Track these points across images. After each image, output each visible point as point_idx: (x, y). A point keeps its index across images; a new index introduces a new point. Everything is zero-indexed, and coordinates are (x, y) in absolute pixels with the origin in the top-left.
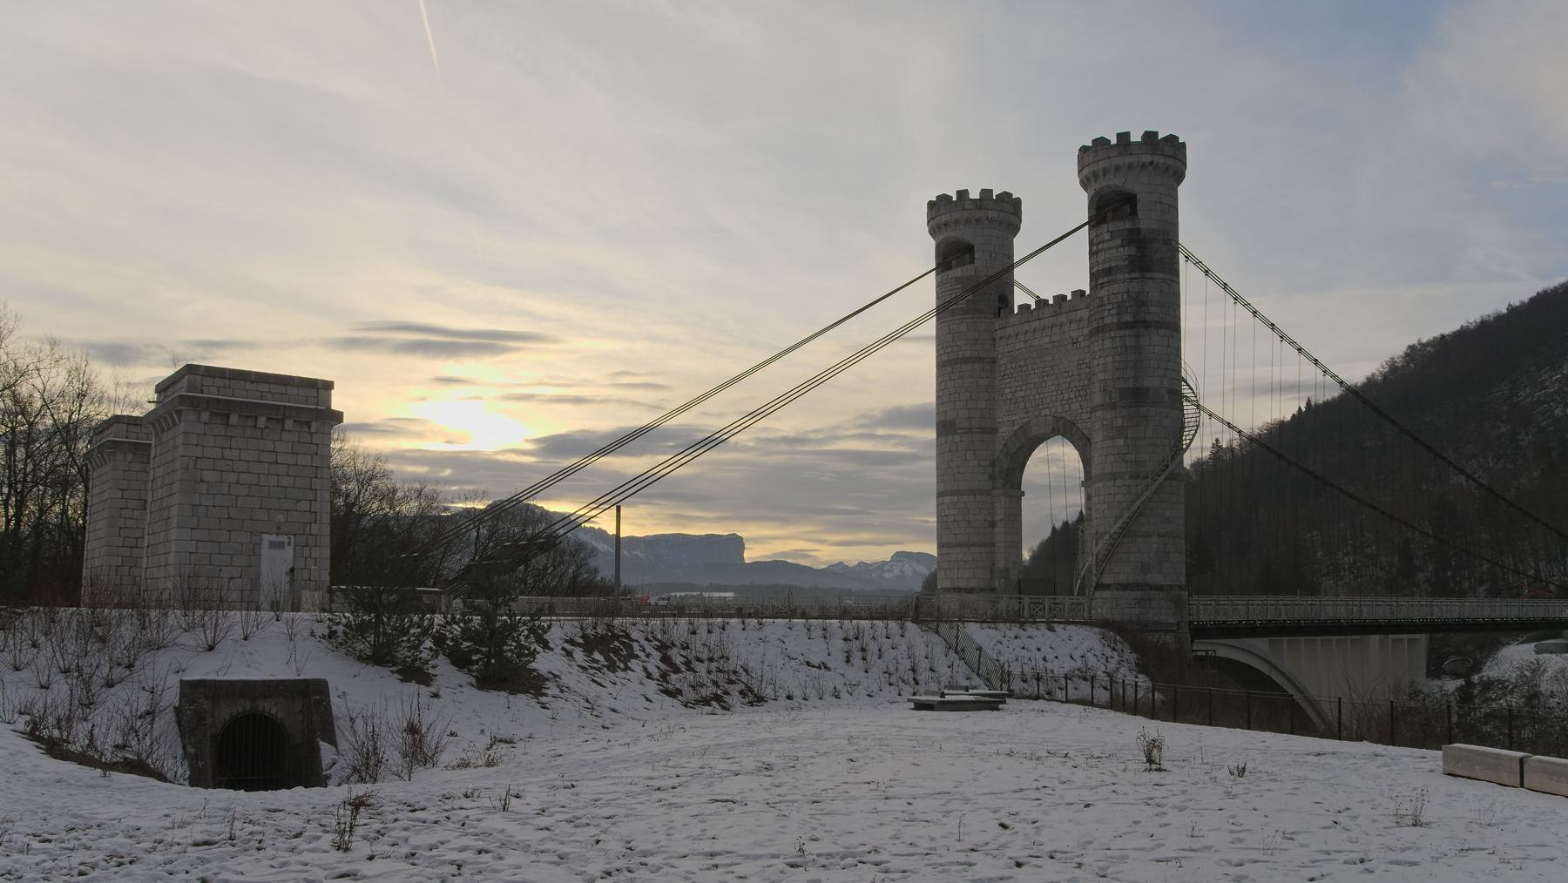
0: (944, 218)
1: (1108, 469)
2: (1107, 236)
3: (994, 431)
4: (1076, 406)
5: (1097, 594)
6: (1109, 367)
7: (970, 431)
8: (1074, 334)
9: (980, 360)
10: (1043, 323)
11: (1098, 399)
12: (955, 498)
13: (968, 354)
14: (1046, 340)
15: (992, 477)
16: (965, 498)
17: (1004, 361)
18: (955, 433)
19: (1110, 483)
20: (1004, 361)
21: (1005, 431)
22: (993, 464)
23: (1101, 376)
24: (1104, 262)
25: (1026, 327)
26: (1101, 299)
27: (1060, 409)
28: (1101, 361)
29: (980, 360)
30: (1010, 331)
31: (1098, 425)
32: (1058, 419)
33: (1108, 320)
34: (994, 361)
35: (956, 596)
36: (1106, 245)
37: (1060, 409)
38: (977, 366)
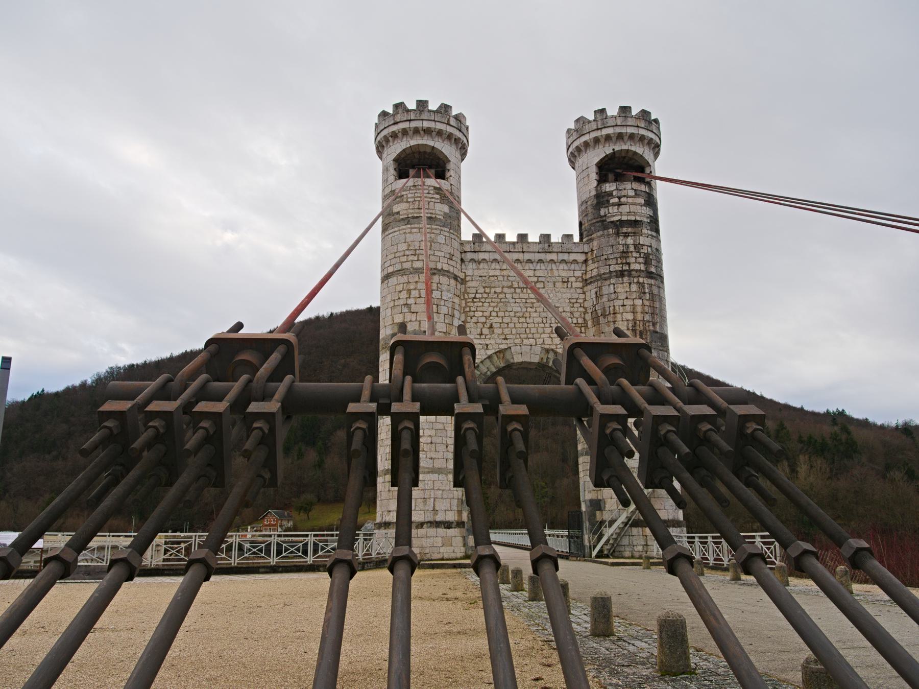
0: (426, 124)
2: (632, 193)
5: (635, 531)
6: (639, 309)
8: (565, 274)
13: (446, 268)
14: (531, 273)
23: (630, 316)
24: (629, 213)
27: (548, 341)
28: (627, 302)
30: (482, 256)
32: (548, 351)
34: (463, 282)
35: (432, 531)
36: (630, 200)
37: (548, 341)
38: (453, 282)
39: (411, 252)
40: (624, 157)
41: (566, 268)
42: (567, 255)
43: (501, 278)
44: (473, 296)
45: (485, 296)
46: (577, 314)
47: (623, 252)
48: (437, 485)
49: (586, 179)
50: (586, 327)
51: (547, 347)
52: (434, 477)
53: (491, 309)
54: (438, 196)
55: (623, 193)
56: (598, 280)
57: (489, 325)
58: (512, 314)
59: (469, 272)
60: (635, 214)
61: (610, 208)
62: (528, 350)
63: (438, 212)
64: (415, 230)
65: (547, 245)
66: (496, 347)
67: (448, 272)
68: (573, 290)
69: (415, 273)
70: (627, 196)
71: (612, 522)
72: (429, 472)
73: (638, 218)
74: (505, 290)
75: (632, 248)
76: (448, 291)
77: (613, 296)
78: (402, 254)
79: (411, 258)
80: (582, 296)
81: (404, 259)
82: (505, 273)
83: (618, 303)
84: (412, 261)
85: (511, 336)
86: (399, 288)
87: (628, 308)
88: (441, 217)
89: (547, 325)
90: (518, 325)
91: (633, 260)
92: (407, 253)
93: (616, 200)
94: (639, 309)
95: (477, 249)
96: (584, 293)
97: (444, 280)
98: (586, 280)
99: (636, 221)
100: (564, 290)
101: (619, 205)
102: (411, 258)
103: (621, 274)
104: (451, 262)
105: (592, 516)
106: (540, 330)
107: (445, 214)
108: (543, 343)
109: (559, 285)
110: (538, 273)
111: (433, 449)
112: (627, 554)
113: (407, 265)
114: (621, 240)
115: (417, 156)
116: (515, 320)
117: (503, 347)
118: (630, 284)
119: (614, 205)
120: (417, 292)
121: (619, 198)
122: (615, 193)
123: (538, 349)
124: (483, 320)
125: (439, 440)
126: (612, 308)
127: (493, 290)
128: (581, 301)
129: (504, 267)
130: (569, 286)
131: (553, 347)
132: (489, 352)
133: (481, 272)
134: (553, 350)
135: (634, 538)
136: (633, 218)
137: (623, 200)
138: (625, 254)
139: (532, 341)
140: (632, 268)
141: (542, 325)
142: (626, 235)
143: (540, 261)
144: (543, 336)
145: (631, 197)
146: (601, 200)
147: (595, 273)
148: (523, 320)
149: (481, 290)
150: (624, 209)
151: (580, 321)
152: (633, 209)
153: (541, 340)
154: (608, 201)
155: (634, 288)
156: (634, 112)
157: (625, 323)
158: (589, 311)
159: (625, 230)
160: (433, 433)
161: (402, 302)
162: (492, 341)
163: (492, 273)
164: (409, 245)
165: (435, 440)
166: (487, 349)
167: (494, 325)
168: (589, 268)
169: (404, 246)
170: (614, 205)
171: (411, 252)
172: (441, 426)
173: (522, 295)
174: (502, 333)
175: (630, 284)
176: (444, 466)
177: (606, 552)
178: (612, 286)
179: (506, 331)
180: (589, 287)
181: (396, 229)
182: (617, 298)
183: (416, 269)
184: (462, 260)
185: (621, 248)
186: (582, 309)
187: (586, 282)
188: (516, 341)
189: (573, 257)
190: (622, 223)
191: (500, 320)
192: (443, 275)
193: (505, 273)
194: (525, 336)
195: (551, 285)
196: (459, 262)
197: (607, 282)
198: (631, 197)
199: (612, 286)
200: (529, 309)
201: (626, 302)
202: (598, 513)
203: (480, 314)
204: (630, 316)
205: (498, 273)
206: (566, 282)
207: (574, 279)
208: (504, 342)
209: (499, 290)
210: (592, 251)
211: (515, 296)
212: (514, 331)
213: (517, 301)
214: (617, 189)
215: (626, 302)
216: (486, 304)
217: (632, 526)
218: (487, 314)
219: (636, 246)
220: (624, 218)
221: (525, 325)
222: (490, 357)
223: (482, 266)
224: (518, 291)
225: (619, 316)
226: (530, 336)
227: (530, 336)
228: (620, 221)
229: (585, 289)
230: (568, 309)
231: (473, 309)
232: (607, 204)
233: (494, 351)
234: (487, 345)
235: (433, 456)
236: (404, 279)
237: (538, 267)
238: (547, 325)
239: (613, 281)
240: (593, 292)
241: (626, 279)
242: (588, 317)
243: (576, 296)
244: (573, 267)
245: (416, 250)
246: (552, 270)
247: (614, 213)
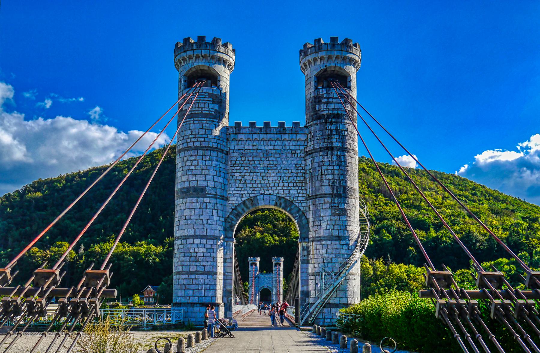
1: (335, 233)
3: (225, 199)
4: (295, 192)
5: (326, 310)
7: (215, 196)
8: (293, 148)
9: (222, 151)
10: (269, 136)
11: (327, 190)
12: (204, 241)
13: (215, 145)
14: (271, 147)
15: (225, 230)
16: (211, 242)
17: (235, 155)
18: (205, 197)
19: (337, 242)
20: (235, 155)
21: (234, 201)
22: (226, 220)
23: (330, 177)
24: (333, 110)
25: (255, 136)
26: (331, 131)
28: (330, 168)
29: (222, 151)
30: (240, 137)
31: (327, 206)
32: (280, 198)
33: (336, 144)
34: (227, 154)
36: (334, 100)
38: (220, 155)
39: (193, 136)
40: (334, 71)
41: (294, 144)
42: (295, 135)
43: (252, 151)
44: (234, 162)
45: (242, 162)
46: (300, 175)
48: (207, 281)
49: (309, 85)
50: (306, 183)
51: (281, 195)
52: (205, 277)
53: (245, 171)
54: (211, 100)
55: (331, 96)
57: (244, 182)
58: (259, 174)
59: (232, 147)
60: (338, 109)
61: (322, 105)
62: (268, 198)
63: (211, 110)
64: (196, 122)
65: (282, 129)
66: (248, 195)
67: (217, 148)
68: (298, 159)
69: (195, 149)
70: (332, 98)
71: (312, 304)
72: (201, 274)
73: (339, 112)
74: (255, 159)
75: (334, 133)
76: (217, 160)
77: (321, 164)
78: (188, 137)
79: (193, 140)
80: (303, 162)
81: (189, 140)
82: (255, 147)
83: (325, 168)
84: (194, 142)
85: (258, 189)
86: (186, 159)
87: (330, 172)
88: (213, 113)
89: (281, 181)
90: (262, 182)
91: (334, 140)
92: (191, 136)
93: (326, 100)
94: (336, 172)
96: (305, 160)
97: (214, 154)
98: (307, 152)
99: (338, 114)
100: (293, 159)
101: (328, 103)
102: (193, 140)
103: (327, 149)
104: (219, 142)
105: (304, 300)
106: (276, 185)
107: (216, 110)
108: (278, 193)
109: (289, 155)
110: (276, 148)
111: (204, 260)
112: (321, 323)
113: (190, 145)
114: (328, 126)
115: (200, 72)
116: (260, 178)
117: (251, 195)
118: (332, 155)
119: (325, 103)
120: (196, 162)
121: (328, 98)
122: (325, 96)
123: (274, 198)
124: (240, 178)
125: (209, 254)
126: (320, 172)
127: (247, 159)
128: (303, 166)
129: (255, 144)
130: (296, 156)
131: (283, 196)
132: (243, 199)
133: (239, 147)
134: (283, 198)
135: (326, 314)
136: (336, 112)
137: (330, 100)
138: (329, 137)
139: (271, 192)
140: (334, 145)
141: (277, 181)
142: (331, 123)
143: (277, 140)
144: (278, 188)
145: (336, 98)
146: (317, 100)
148: (265, 178)
149: (240, 159)
150: (332, 106)
151: (302, 178)
152: (336, 106)
153: (276, 192)
154: (321, 101)
155: (335, 158)
156: (340, 41)
157: (328, 181)
158: (308, 172)
159: (330, 120)
160: (204, 250)
161: (187, 168)
162: (246, 192)
163: (246, 147)
164: (192, 132)
165: (205, 254)
166: (242, 197)
167: (247, 182)
168: (309, 144)
169: (189, 132)
170: (325, 103)
171: (193, 136)
172: (209, 246)
173: (265, 162)
174: (252, 187)
175: (332, 155)
176: (211, 270)
177: (310, 322)
178: (321, 157)
179: (255, 185)
180: (308, 157)
182: (323, 165)
183: (196, 147)
184: (227, 139)
186: (303, 171)
187: (307, 153)
188: (261, 192)
189: (299, 136)
190: (329, 116)
191: (251, 178)
192: (213, 150)
194: (267, 189)
195: (284, 156)
196: (225, 140)
197: (318, 154)
198: (336, 98)
199: (321, 157)
200: (270, 171)
201: (329, 168)
202: (307, 298)
203: (238, 174)
204: (330, 177)
205: (250, 147)
206: (293, 153)
207: (299, 151)
208: (253, 192)
209: (250, 159)
210: (311, 133)
211: (261, 162)
212: (259, 186)
213: (262, 166)
214: (326, 93)
215: (329, 168)
216: (242, 168)
217: (324, 307)
218: (243, 174)
219: (337, 130)
220: (330, 112)
221: (267, 182)
222: (244, 203)
223: (240, 143)
224: (263, 159)
225: (324, 177)
226: (270, 188)
227: (270, 188)
229: (306, 158)
230: (294, 171)
231: (234, 171)
232: (320, 102)
233: (246, 198)
234: (242, 195)
235: (205, 264)
236: (188, 153)
237: (276, 144)
238: (281, 181)
239: (321, 154)
240: (310, 159)
241: (330, 152)
242: (307, 176)
243: (300, 162)
244: (299, 143)
245: (196, 135)
246: (285, 145)
247: (324, 109)
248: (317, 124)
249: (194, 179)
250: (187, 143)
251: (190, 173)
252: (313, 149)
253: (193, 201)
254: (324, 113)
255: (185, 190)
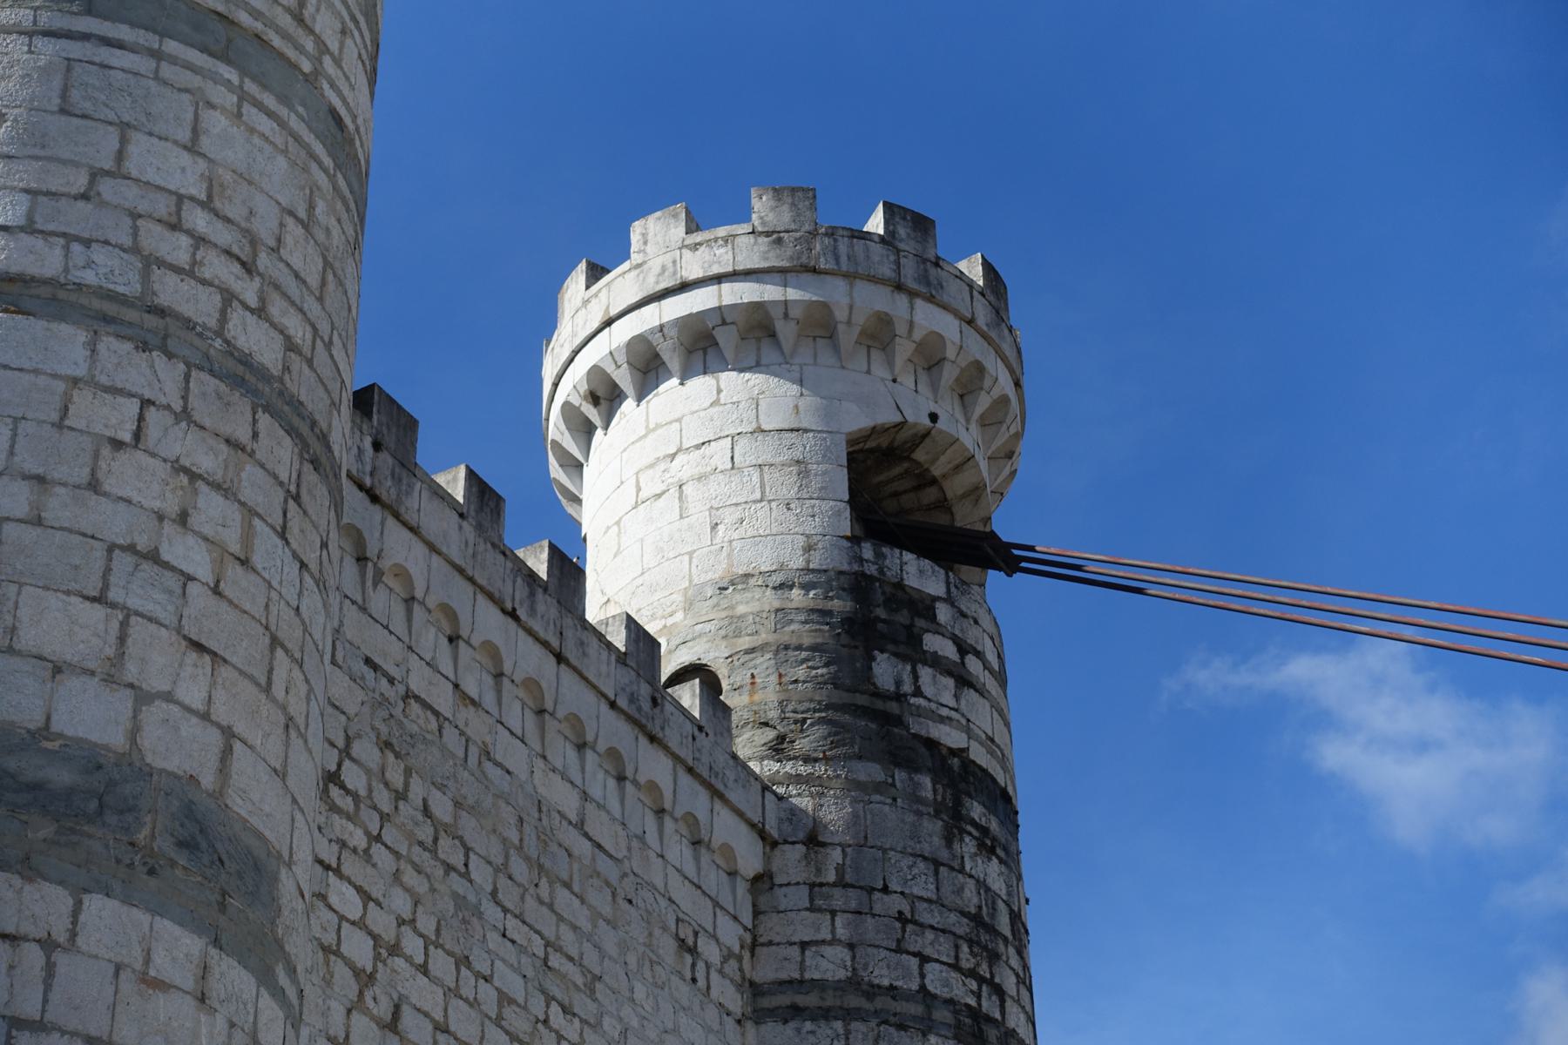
47: (976, 919)
56: (849, 1015)
57: (384, 1010)
69: (237, 382)
78: (163, 206)
81: (177, 249)
82: (477, 725)
86: (119, 418)
95: (387, 490)
119: (936, 662)
121: (963, 649)
122: (943, 613)
147: (830, 965)
161: (116, 524)
181: (124, 32)
185: (971, 899)
193: (477, 725)
209: (442, 808)
228: (960, 753)
248: (878, 788)
249: (194, 695)
250: (151, 262)
251: (140, 591)
252: (854, 983)
253: (162, 966)
254: (952, 738)
255: (61, 776)
